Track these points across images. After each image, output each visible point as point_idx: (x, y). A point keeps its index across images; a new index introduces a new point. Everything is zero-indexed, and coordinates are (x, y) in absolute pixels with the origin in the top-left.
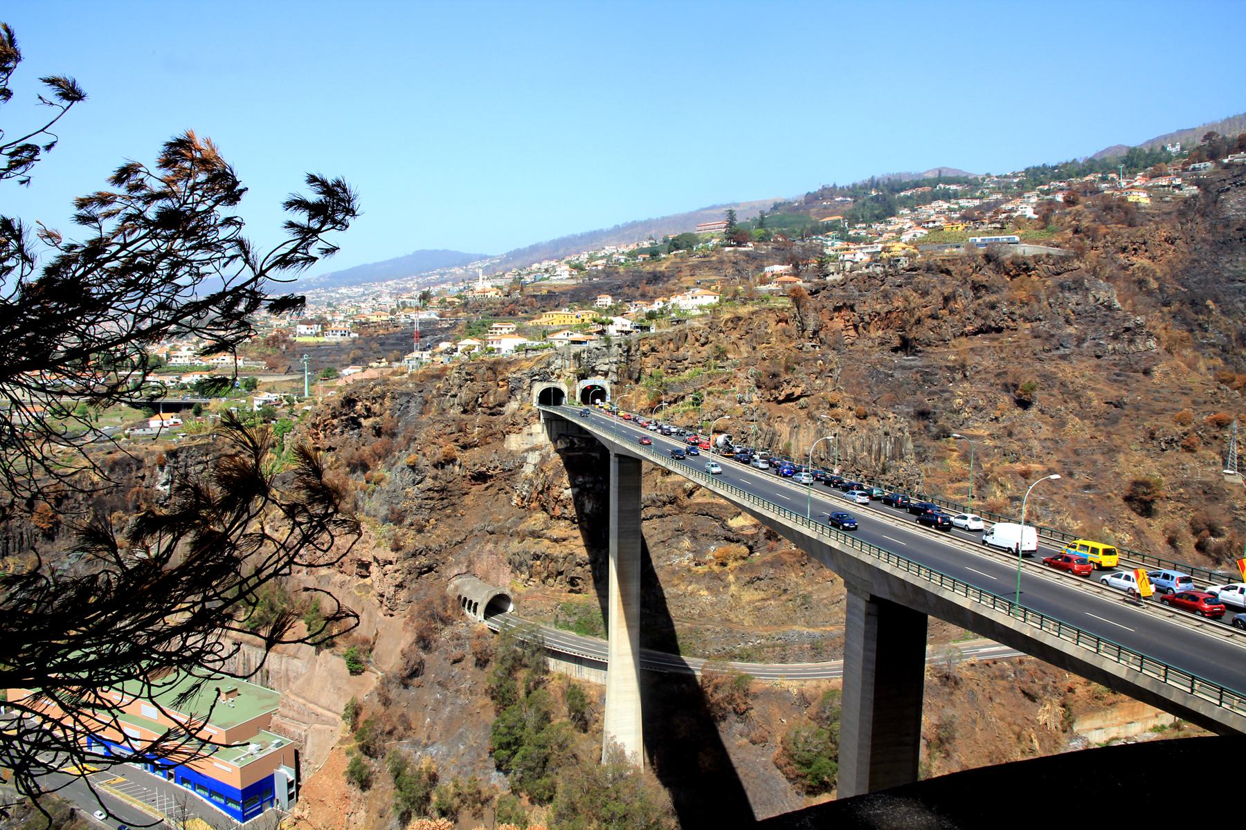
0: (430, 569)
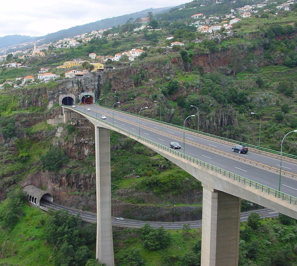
0: (15, 183)
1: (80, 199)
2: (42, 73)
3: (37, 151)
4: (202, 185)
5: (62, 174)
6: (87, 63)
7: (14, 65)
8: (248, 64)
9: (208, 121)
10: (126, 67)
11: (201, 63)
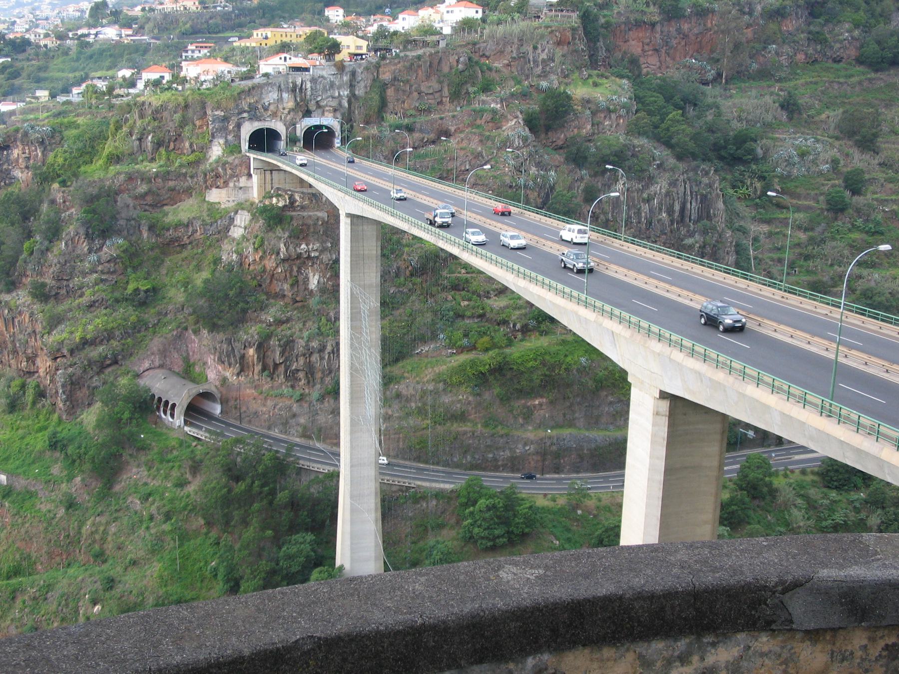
0: (115, 362)
1: (295, 407)
2: (193, 59)
3: (179, 276)
4: (629, 380)
5: (247, 340)
6: (322, 34)
7: (110, 33)
8: (763, 56)
9: (645, 208)
10: (429, 50)
11: (634, 47)
